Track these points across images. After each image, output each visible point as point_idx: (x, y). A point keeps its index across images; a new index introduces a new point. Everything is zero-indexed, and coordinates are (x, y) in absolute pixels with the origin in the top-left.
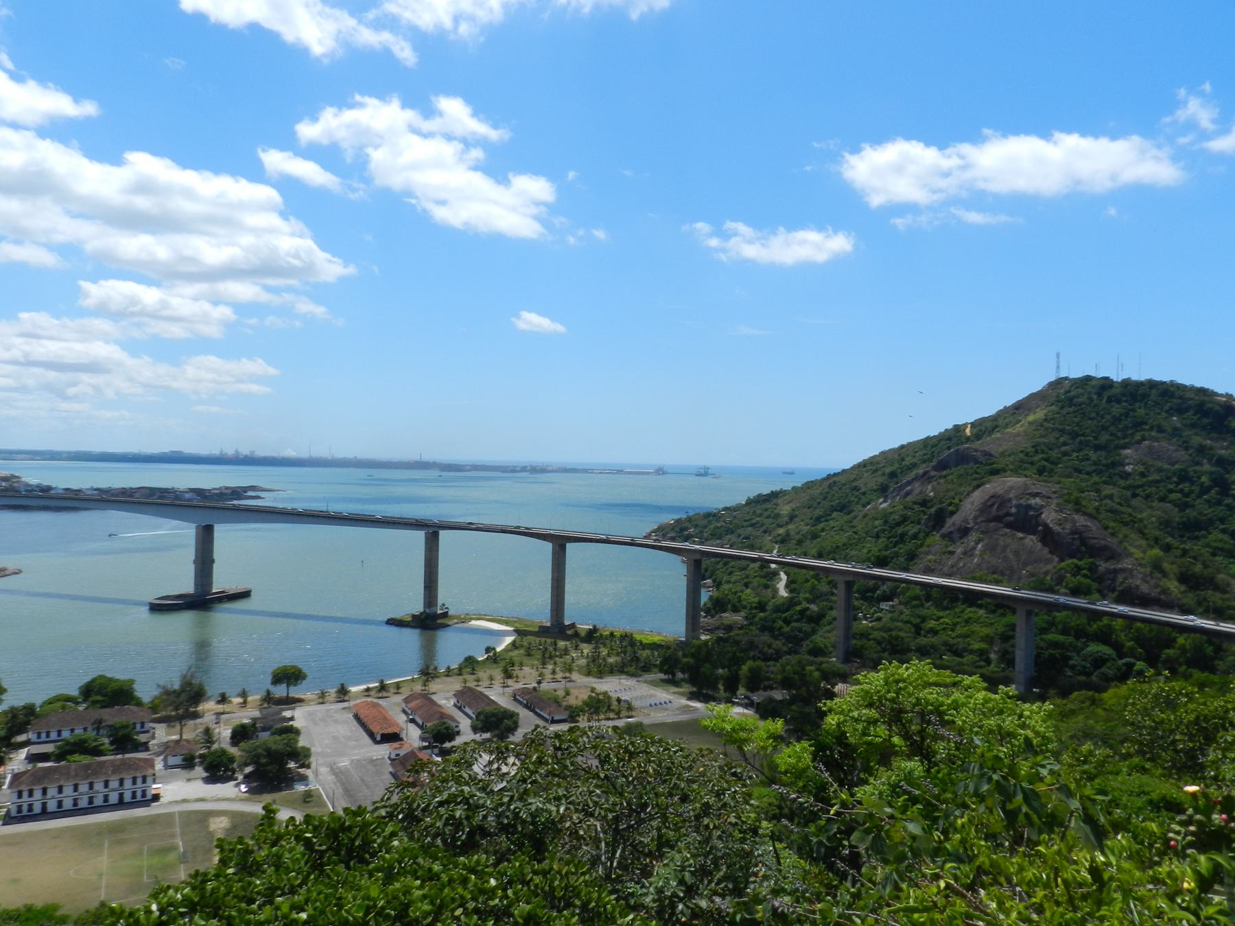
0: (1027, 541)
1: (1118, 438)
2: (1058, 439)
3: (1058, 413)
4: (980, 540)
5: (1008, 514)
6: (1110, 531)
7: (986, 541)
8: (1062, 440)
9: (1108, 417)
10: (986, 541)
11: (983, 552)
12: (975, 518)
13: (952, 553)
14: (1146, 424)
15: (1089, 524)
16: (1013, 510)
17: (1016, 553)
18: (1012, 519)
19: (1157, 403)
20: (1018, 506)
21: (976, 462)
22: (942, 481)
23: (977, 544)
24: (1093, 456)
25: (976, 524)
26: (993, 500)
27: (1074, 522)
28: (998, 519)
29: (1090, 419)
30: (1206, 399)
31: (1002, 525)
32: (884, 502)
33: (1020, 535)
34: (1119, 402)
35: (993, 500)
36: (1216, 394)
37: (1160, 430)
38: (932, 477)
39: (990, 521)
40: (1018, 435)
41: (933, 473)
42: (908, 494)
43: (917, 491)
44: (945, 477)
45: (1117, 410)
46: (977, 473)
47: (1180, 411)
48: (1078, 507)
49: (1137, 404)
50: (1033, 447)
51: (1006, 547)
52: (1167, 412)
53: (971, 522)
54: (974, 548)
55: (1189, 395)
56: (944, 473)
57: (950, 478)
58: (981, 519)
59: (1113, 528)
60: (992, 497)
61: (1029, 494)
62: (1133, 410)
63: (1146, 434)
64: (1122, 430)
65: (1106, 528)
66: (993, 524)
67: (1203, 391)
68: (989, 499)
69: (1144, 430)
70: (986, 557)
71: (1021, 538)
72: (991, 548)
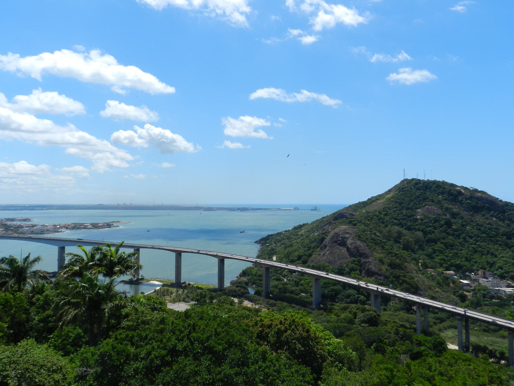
0: (343, 250)
1: (417, 205)
2: (394, 205)
3: (397, 195)
4: (328, 250)
5: (339, 240)
6: (369, 247)
7: (330, 251)
8: (395, 205)
9: (414, 196)
10: (330, 251)
11: (328, 254)
12: (329, 241)
13: (320, 254)
14: (428, 199)
15: (361, 244)
16: (340, 239)
17: (338, 256)
18: (340, 242)
19: (434, 190)
20: (342, 237)
21: (346, 217)
22: (334, 225)
23: (327, 251)
24: (405, 212)
25: (329, 243)
26: (335, 235)
27: (356, 243)
28: (335, 242)
29: (408, 197)
30: (452, 188)
31: (336, 244)
32: (317, 232)
33: (341, 248)
34: (420, 190)
35: (335, 235)
36: (457, 186)
37: (433, 201)
38: (332, 223)
39: (333, 243)
40: (380, 204)
41: (333, 222)
42: (324, 229)
43: (326, 229)
44: (336, 223)
45: (418, 193)
46: (345, 222)
47: (442, 193)
48: (359, 238)
49: (427, 191)
50: (383, 208)
51: (335, 253)
52: (437, 194)
53: (327, 243)
54: (326, 253)
55: (446, 187)
56: (336, 222)
57: (337, 224)
58: (330, 242)
59: (371, 246)
60: (335, 233)
61: (346, 233)
62: (425, 193)
63: (427, 203)
64: (419, 201)
65: (368, 246)
66: (334, 244)
67: (452, 185)
68: (334, 234)
69: (427, 201)
70: (328, 256)
71: (341, 249)
72: (331, 253)
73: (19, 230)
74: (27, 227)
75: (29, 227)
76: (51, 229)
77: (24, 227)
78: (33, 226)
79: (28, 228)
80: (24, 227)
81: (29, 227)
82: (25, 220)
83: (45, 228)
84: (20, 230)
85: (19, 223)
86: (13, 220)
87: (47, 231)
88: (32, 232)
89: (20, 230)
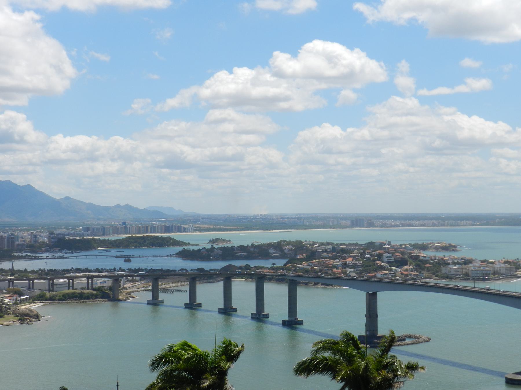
73: (440, 271)
74: (455, 264)
75: (458, 263)
76: (503, 271)
77: (448, 264)
78: (467, 262)
79: (457, 267)
80: (448, 264)
81: (458, 263)
82: (446, 248)
83: (489, 268)
84: (444, 270)
85: (440, 255)
86: (424, 247)
87: (494, 273)
88: (467, 277)
89: (444, 270)
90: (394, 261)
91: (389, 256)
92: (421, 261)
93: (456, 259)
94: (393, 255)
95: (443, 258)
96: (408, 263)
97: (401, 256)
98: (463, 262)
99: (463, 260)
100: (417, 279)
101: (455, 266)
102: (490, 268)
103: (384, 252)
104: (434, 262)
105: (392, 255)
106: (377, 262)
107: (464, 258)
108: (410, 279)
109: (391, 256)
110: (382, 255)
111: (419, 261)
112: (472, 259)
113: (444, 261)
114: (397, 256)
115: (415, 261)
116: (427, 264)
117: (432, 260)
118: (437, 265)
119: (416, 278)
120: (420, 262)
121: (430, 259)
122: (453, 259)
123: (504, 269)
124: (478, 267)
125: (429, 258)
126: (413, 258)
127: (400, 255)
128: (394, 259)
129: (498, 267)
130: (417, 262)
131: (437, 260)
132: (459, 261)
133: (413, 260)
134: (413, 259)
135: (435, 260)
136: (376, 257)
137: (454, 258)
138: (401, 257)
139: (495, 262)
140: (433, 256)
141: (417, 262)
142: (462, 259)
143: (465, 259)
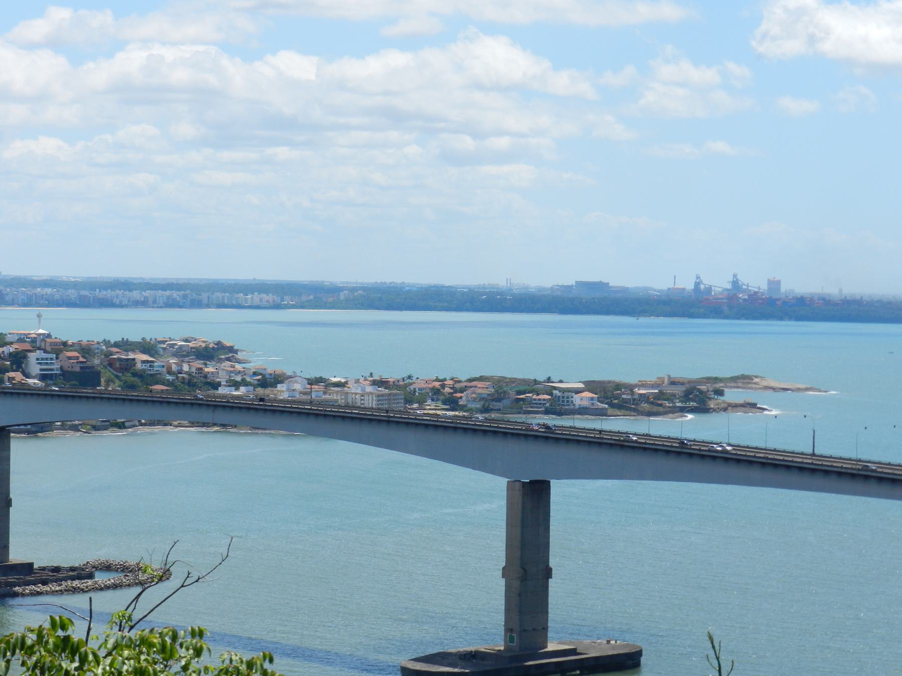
90: (60, 375)
91: (47, 359)
92: (139, 375)
93: (239, 372)
94: (57, 358)
95: (201, 369)
96: (102, 380)
97: (81, 359)
98: (258, 380)
99: (260, 377)
100: (127, 424)
101: (237, 389)
102: (335, 395)
103: (32, 349)
104: (177, 378)
105: (55, 355)
106: (12, 374)
107: (261, 372)
108: (106, 423)
109: (52, 359)
110: (25, 357)
111: (132, 373)
112: (284, 374)
113: (205, 377)
114: (69, 358)
115: (120, 374)
116: (157, 383)
117: (170, 372)
118: (186, 387)
119: (123, 423)
120: (136, 378)
121: (164, 370)
122: (231, 372)
123: (374, 398)
124: (301, 393)
125: (163, 366)
126: (118, 365)
127: (77, 358)
128: (61, 368)
129: (356, 394)
130: (129, 377)
131: (186, 373)
132: (248, 379)
133: (115, 373)
134: (116, 369)
135: (181, 373)
136: (8, 363)
137: (232, 369)
138: (82, 362)
139: (346, 383)
140: (174, 363)
141: (129, 377)
142: (255, 374)
143: (263, 376)
